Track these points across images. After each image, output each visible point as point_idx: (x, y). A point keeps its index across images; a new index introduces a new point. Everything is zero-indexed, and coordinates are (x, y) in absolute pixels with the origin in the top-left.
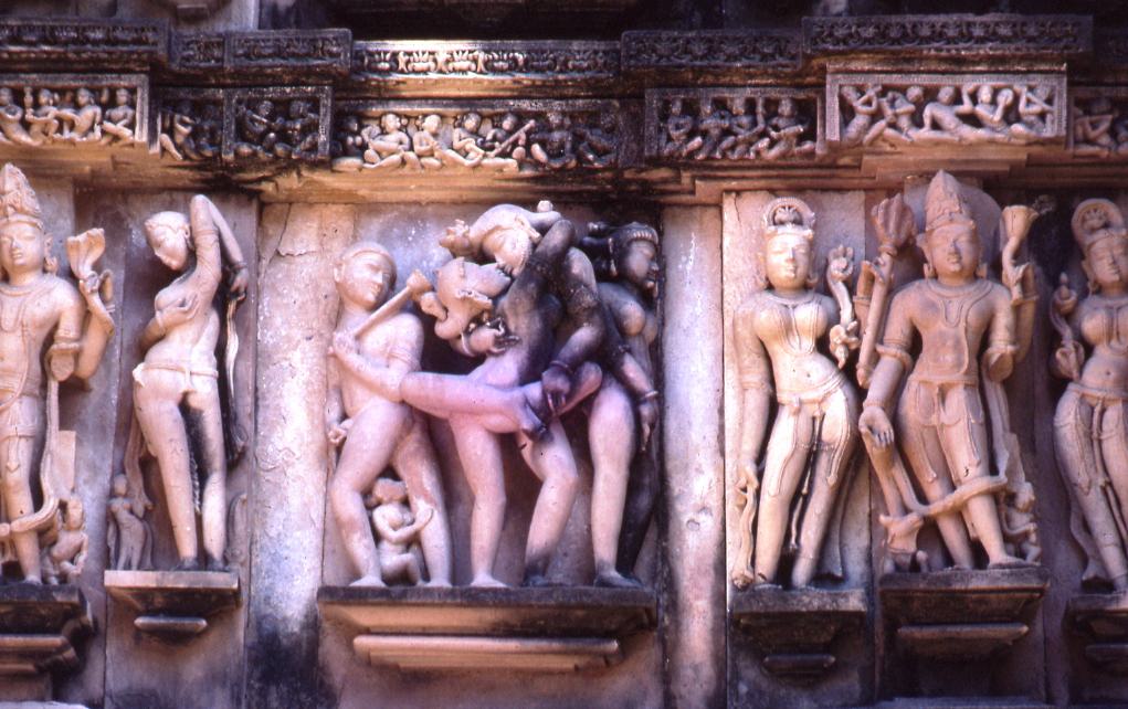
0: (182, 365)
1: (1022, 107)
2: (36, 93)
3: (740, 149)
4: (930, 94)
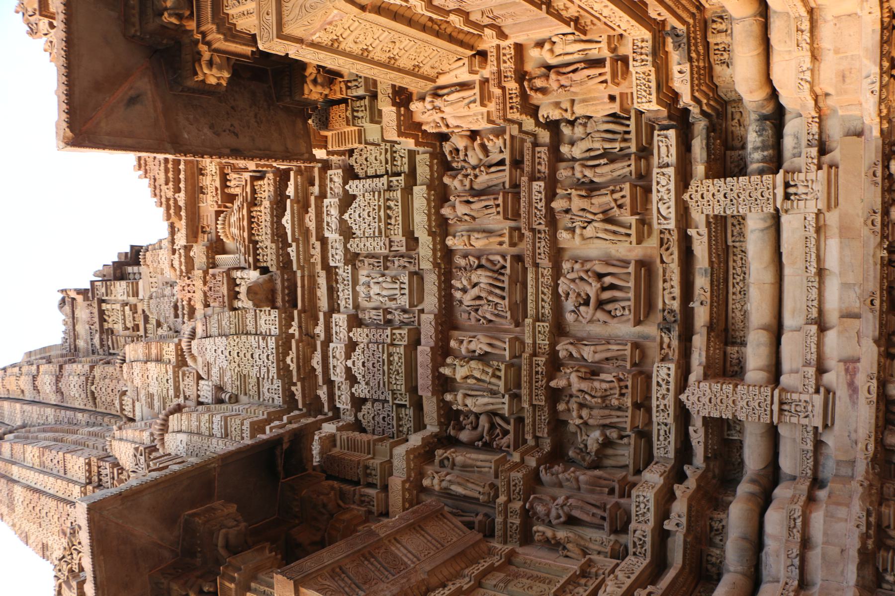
0: (588, 353)
4: (536, 208)
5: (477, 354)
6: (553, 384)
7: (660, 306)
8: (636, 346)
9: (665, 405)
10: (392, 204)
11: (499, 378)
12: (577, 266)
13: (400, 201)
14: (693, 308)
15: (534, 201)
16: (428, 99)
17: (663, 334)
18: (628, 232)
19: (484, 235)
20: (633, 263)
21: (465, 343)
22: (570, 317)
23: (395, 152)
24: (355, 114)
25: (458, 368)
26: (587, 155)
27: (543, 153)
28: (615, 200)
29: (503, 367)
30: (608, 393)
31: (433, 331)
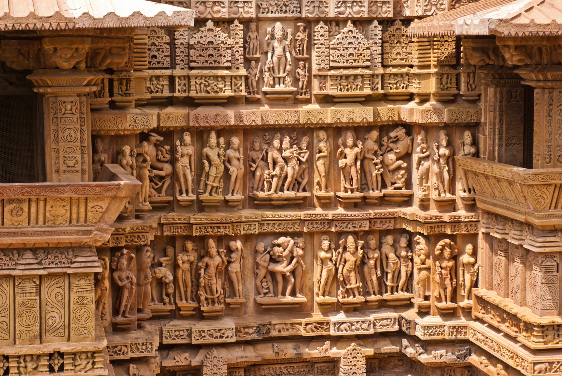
4: (349, 223)
9: (205, 337)
17: (255, 328)
24: (445, 76)
26: (384, 258)
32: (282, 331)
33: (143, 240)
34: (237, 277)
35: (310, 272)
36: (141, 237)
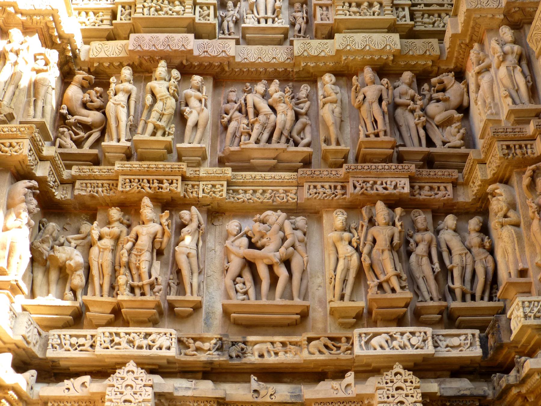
1: (398, 186)
2: (153, 181)
3: (327, 197)
4: (375, 183)
5: (183, 108)
6: (146, 201)
7: (250, 338)
8: (197, 307)
9: (119, 344)
10: (376, 8)
11: (154, 134)
12: (299, 234)
13: (380, 17)
14: (249, 381)
15: (384, 180)
16: (516, 48)
17: (214, 341)
18: (346, 297)
19: (338, 120)
20: (306, 303)
21: (198, 94)
22: (233, 225)
23: (439, 16)
25: (166, 84)
26: (444, 248)
27: (445, 193)
28: (388, 281)
29: (169, 138)
30: (134, 271)
31: (213, 54)
32: (266, 354)
33: (17, 148)
34: (190, 263)
35: (319, 275)
36: (14, 144)
